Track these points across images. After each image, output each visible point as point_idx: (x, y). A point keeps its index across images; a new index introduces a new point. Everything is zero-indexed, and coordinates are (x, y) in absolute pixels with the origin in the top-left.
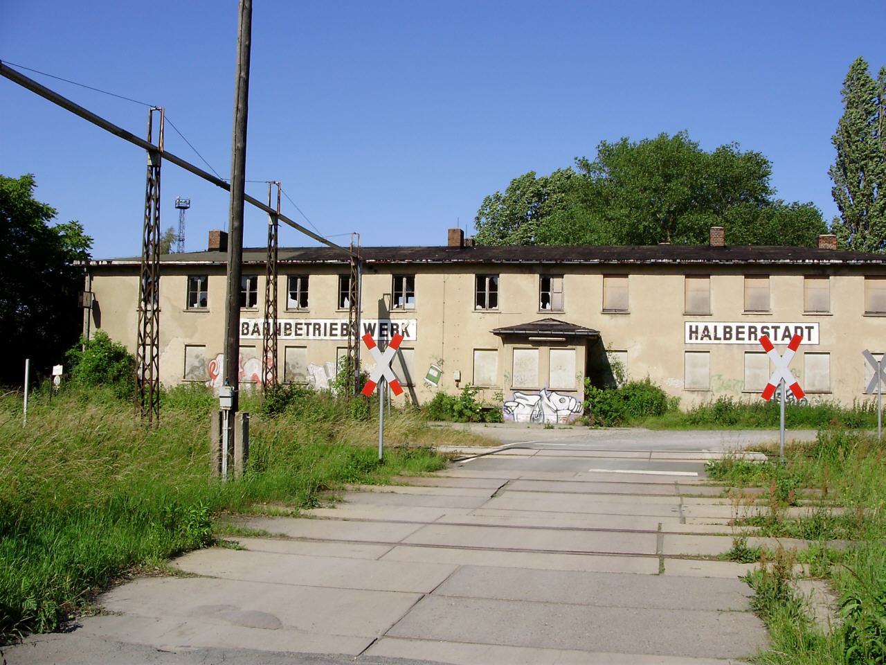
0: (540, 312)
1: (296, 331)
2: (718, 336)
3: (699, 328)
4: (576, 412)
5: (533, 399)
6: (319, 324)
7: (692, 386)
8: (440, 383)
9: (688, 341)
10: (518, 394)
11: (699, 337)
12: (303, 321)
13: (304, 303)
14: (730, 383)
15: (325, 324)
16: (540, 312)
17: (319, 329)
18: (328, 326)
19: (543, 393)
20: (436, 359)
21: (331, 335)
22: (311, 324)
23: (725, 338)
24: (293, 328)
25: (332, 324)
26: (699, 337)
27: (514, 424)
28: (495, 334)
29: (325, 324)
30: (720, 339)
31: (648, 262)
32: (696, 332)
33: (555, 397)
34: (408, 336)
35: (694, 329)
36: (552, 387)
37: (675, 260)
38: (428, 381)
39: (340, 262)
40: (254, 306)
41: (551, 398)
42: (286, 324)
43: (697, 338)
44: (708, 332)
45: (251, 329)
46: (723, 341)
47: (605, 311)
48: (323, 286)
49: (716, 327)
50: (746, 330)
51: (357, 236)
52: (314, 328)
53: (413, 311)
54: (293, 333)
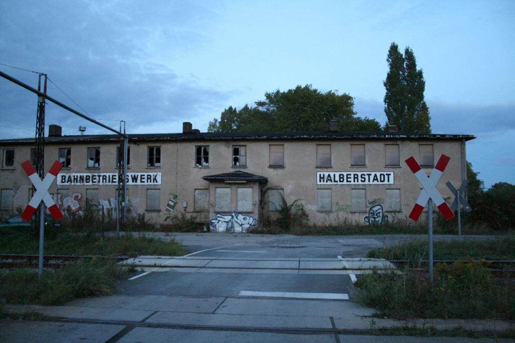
0: (233, 167)
1: (92, 180)
2: (336, 180)
3: (325, 175)
4: (253, 225)
5: (228, 218)
6: (106, 176)
7: (322, 209)
8: (175, 209)
9: (319, 183)
10: (219, 215)
11: (325, 181)
12: (96, 174)
13: (97, 160)
14: (343, 207)
15: (109, 176)
16: (233, 167)
17: (105, 179)
18: (111, 177)
19: (233, 214)
20: (173, 195)
21: (113, 182)
22: (101, 176)
23: (340, 181)
24: (91, 179)
25: (141, 176)
26: (325, 181)
27: (216, 232)
28: (204, 179)
29: (109, 176)
30: (337, 182)
31: (295, 137)
32: (323, 178)
33: (241, 217)
34: (157, 182)
35: (322, 176)
36: (240, 209)
37: (311, 136)
38: (168, 208)
39: (117, 140)
40: (69, 166)
41: (238, 217)
42: (87, 176)
43: (324, 181)
44: (330, 177)
45: (67, 179)
46: (339, 183)
47: (271, 167)
48: (109, 153)
49: (334, 175)
50: (146, 177)
51: (123, 123)
52: (103, 179)
53: (159, 167)
54: (91, 182)
